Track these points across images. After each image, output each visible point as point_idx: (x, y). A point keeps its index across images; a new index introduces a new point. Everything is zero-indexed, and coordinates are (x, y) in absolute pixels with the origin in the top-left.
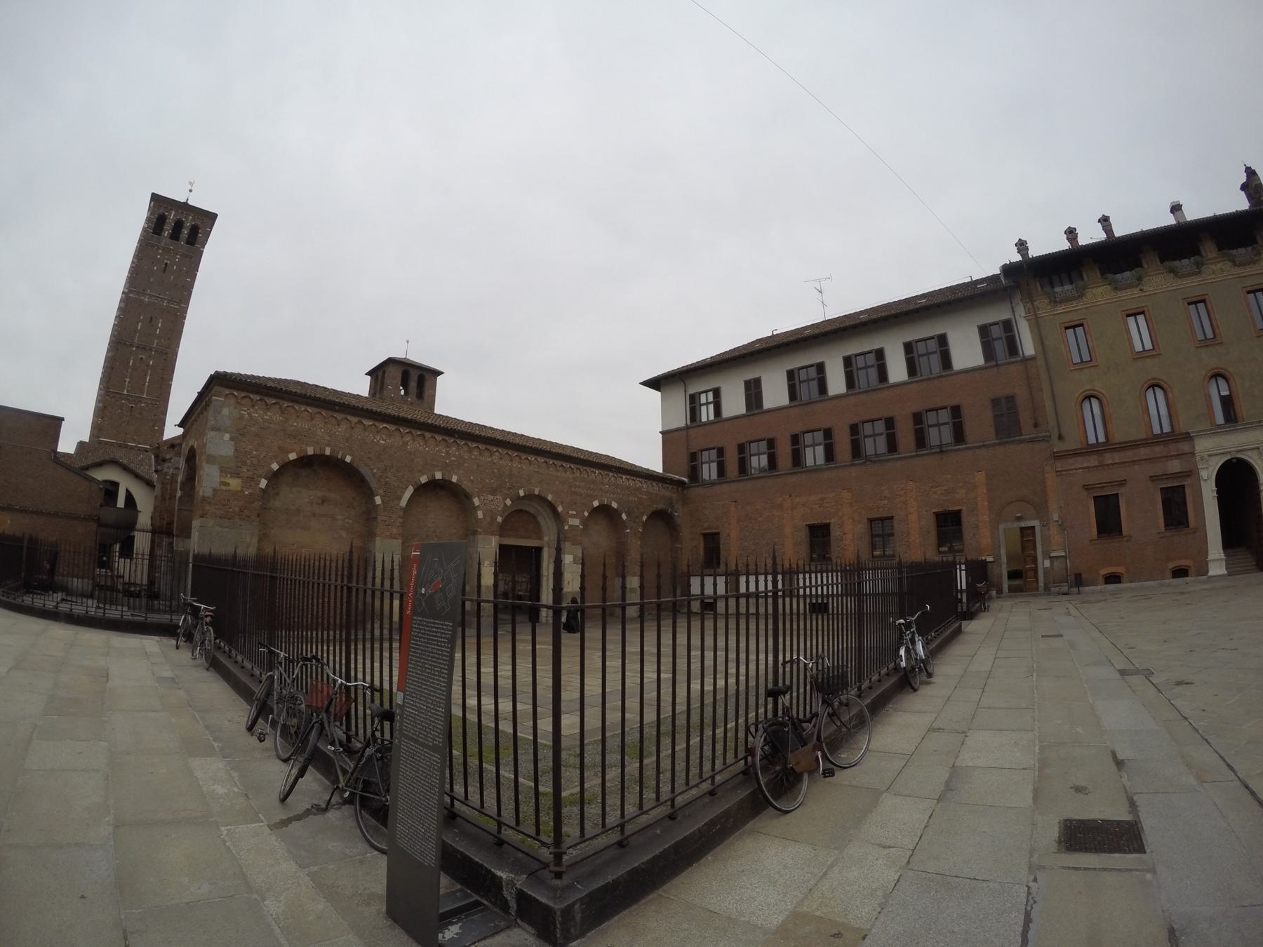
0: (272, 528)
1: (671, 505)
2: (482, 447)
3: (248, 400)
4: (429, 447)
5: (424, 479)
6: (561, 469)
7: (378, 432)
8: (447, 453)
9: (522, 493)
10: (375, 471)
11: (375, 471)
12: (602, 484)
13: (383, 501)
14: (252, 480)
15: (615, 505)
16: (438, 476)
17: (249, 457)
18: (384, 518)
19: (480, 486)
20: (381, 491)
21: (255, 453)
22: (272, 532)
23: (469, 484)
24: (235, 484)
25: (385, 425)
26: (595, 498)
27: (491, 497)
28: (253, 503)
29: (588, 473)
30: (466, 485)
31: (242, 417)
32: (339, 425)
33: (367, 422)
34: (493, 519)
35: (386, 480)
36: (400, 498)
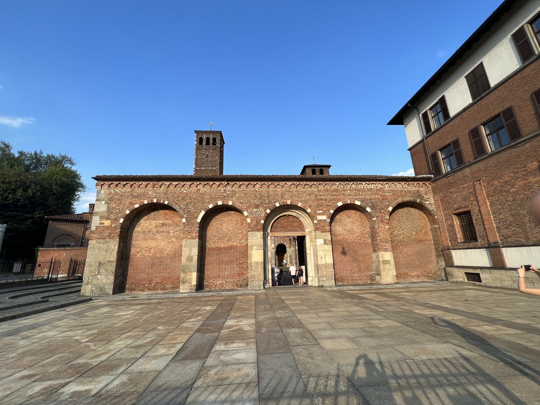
0: (136, 241)
1: (420, 196)
2: (246, 183)
3: (114, 185)
4: (213, 189)
5: (211, 206)
6: (306, 186)
7: (183, 187)
8: (225, 190)
9: (277, 205)
10: (182, 206)
11: (182, 206)
12: (344, 191)
13: (187, 221)
14: (116, 219)
15: (358, 203)
16: (220, 203)
17: (114, 209)
18: (188, 229)
19: (248, 205)
20: (185, 216)
21: (117, 207)
22: (136, 242)
23: (240, 205)
24: (107, 223)
25: (185, 183)
26: (339, 200)
27: (255, 210)
28: (116, 230)
29: (330, 186)
30: (238, 205)
31: (110, 193)
32: (160, 187)
33: (175, 183)
34: (258, 222)
35: (188, 209)
36: (197, 218)
